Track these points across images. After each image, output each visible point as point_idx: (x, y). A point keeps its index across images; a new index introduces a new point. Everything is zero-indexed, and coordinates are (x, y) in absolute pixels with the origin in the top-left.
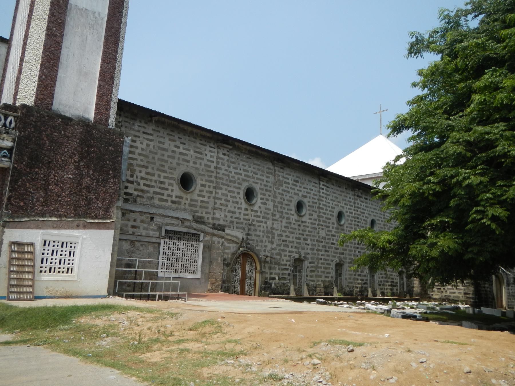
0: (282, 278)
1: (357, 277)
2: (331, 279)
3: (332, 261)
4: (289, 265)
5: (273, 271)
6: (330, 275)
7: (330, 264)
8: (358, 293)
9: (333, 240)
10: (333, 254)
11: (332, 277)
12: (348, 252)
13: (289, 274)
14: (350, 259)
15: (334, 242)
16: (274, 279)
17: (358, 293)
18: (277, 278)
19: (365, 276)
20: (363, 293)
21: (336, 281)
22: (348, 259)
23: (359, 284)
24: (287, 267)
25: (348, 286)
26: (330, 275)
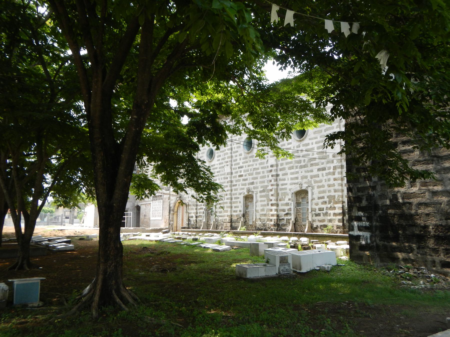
0: (200, 216)
1: (270, 207)
2: (240, 213)
3: (240, 194)
4: (203, 205)
5: (192, 211)
6: (238, 209)
7: (238, 198)
8: (272, 227)
9: (241, 172)
10: (241, 187)
11: (240, 211)
12: (259, 180)
13: (203, 212)
14: (262, 187)
15: (242, 173)
16: (192, 217)
17: (272, 227)
18: (194, 216)
19: (287, 204)
20: (284, 228)
21: (244, 215)
22: (260, 187)
23: (272, 215)
24: (202, 207)
25: (260, 219)
26: (238, 209)
